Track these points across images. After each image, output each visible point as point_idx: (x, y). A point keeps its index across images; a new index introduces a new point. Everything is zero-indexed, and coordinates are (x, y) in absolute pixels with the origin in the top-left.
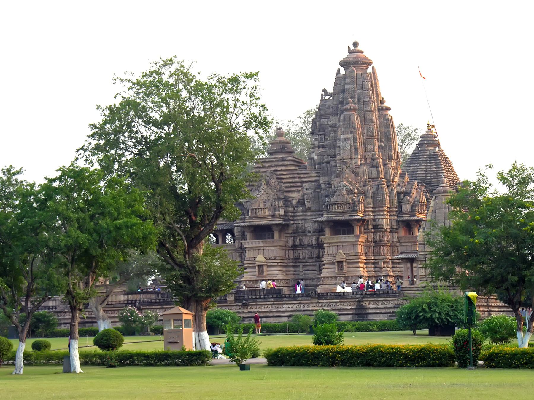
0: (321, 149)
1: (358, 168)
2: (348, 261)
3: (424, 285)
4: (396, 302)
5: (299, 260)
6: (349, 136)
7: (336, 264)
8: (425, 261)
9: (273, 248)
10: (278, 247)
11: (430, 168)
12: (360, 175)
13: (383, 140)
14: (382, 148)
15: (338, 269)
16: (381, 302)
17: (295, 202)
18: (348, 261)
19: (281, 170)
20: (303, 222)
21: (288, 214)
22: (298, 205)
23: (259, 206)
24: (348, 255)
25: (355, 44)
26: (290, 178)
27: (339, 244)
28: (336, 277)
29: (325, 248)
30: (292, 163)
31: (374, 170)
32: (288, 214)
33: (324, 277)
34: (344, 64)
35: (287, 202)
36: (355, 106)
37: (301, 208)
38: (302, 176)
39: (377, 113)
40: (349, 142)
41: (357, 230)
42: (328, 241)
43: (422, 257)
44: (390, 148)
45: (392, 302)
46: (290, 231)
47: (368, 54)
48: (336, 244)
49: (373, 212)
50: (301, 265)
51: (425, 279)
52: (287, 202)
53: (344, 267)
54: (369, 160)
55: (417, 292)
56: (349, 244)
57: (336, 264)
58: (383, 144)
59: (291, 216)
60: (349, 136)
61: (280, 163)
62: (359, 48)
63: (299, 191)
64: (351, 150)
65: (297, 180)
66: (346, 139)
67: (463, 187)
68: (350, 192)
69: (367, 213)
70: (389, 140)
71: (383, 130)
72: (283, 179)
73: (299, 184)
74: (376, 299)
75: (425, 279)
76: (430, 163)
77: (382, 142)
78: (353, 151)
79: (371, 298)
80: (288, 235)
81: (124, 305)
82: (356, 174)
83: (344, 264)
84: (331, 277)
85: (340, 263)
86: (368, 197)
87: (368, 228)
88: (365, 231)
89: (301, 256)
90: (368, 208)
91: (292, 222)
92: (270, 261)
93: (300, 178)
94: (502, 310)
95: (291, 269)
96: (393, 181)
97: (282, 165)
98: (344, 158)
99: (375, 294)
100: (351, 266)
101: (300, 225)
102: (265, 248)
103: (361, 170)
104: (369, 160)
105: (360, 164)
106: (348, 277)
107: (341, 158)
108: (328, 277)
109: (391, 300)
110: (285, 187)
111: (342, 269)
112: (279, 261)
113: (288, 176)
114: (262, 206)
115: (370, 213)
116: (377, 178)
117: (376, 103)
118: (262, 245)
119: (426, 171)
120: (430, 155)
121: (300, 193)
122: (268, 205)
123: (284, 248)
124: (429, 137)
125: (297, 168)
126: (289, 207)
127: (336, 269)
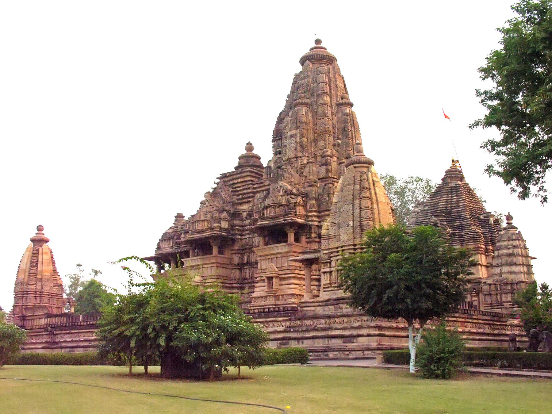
0: (278, 156)
1: (305, 167)
2: (280, 276)
3: (327, 298)
4: (288, 324)
5: (246, 281)
6: (295, 132)
7: (266, 280)
8: (330, 263)
9: (210, 265)
10: (215, 265)
11: (451, 199)
12: (304, 174)
13: (340, 137)
14: (339, 145)
15: (269, 287)
16: (271, 324)
17: (245, 214)
18: (280, 276)
19: (238, 183)
20: (251, 236)
21: (234, 228)
22: (246, 218)
23: (200, 218)
24: (281, 269)
25: (318, 42)
26: (244, 189)
27: (273, 256)
28: (266, 297)
29: (259, 261)
30: (249, 174)
31: (323, 170)
32: (234, 228)
33: (255, 298)
34: (303, 61)
35: (235, 215)
36: (308, 101)
37: (249, 221)
38: (255, 186)
39: (335, 108)
40: (294, 139)
41: (291, 237)
42: (261, 254)
43: (326, 257)
44: (348, 144)
45: (284, 324)
46: (237, 247)
47: (331, 50)
48: (269, 257)
49: (318, 217)
50: (247, 286)
51: (330, 289)
52: (235, 215)
53: (274, 283)
54: (319, 159)
55: (318, 308)
56: (283, 255)
57: (266, 280)
58: (340, 141)
59: (238, 230)
60: (295, 132)
61: (239, 176)
62: (322, 45)
63: (249, 202)
64: (296, 147)
65: (250, 190)
66: (292, 136)
67: (485, 217)
68: (287, 193)
69: (310, 219)
70: (346, 136)
71: (341, 125)
72: (238, 191)
73: (251, 195)
74: (265, 320)
75: (330, 289)
76: (452, 194)
77: (339, 139)
78: (298, 148)
79: (258, 318)
80: (234, 252)
81: (43, 330)
82: (301, 174)
83: (274, 280)
84: (262, 297)
85: (270, 279)
86: (311, 199)
87: (310, 237)
88: (308, 240)
89: (247, 276)
90: (311, 212)
91: (239, 237)
92: (207, 281)
93: (254, 188)
94: (484, 338)
95: (236, 291)
97: (240, 178)
98: (290, 157)
99: (264, 312)
100: (283, 283)
101: (247, 240)
102: (204, 266)
103: (307, 169)
104: (319, 159)
105: (308, 163)
106: (279, 296)
107: (287, 158)
108: (258, 297)
109: (283, 321)
110: (238, 199)
111: (272, 288)
112: (215, 280)
113: (241, 188)
114: (202, 218)
115: (314, 218)
116: (326, 178)
117: (334, 97)
118: (201, 263)
119: (447, 202)
120: (451, 187)
121: (251, 205)
122: (209, 216)
123: (229, 267)
124: (452, 171)
125: (254, 179)
126: (235, 220)
127: (266, 287)
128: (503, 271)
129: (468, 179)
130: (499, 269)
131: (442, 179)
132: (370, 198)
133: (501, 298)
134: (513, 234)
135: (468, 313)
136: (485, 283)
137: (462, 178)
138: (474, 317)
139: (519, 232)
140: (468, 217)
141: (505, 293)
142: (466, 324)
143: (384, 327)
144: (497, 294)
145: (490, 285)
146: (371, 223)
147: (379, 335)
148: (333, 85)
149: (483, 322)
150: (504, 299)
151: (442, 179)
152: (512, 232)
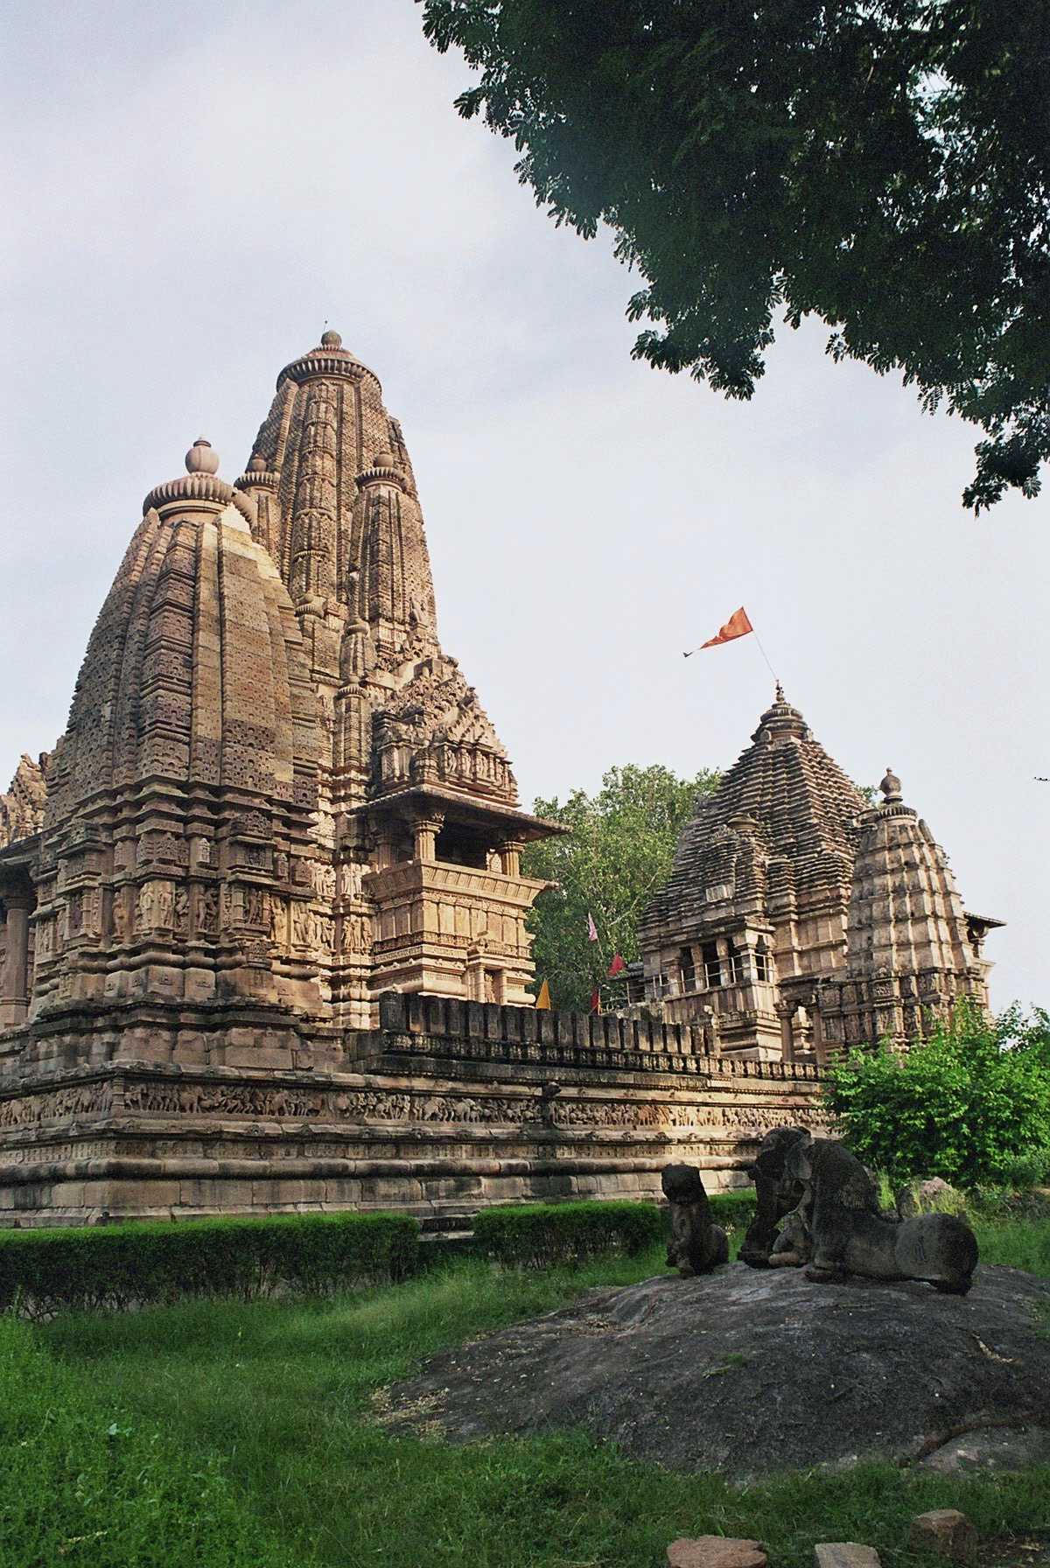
13: (358, 564)
96: (364, 684)
128: (875, 941)
129: (815, 735)
130: (865, 935)
131: (753, 738)
132: (193, 613)
133: (874, 1024)
134: (903, 828)
135: (685, 1070)
136: (827, 981)
137: (802, 732)
138: (714, 1084)
139: (921, 822)
140: (815, 821)
141: (882, 1009)
142: (676, 1109)
143: (154, 1137)
144: (861, 1015)
145: (841, 986)
146: (182, 701)
147: (115, 1173)
148: (350, 432)
149: (762, 1099)
150: (881, 1029)
151: (753, 738)
152: (900, 822)
